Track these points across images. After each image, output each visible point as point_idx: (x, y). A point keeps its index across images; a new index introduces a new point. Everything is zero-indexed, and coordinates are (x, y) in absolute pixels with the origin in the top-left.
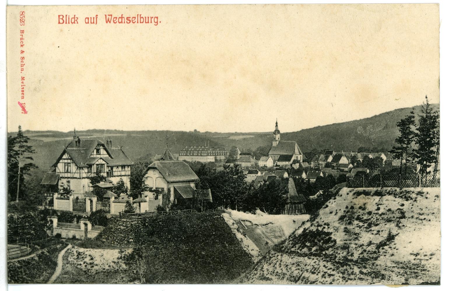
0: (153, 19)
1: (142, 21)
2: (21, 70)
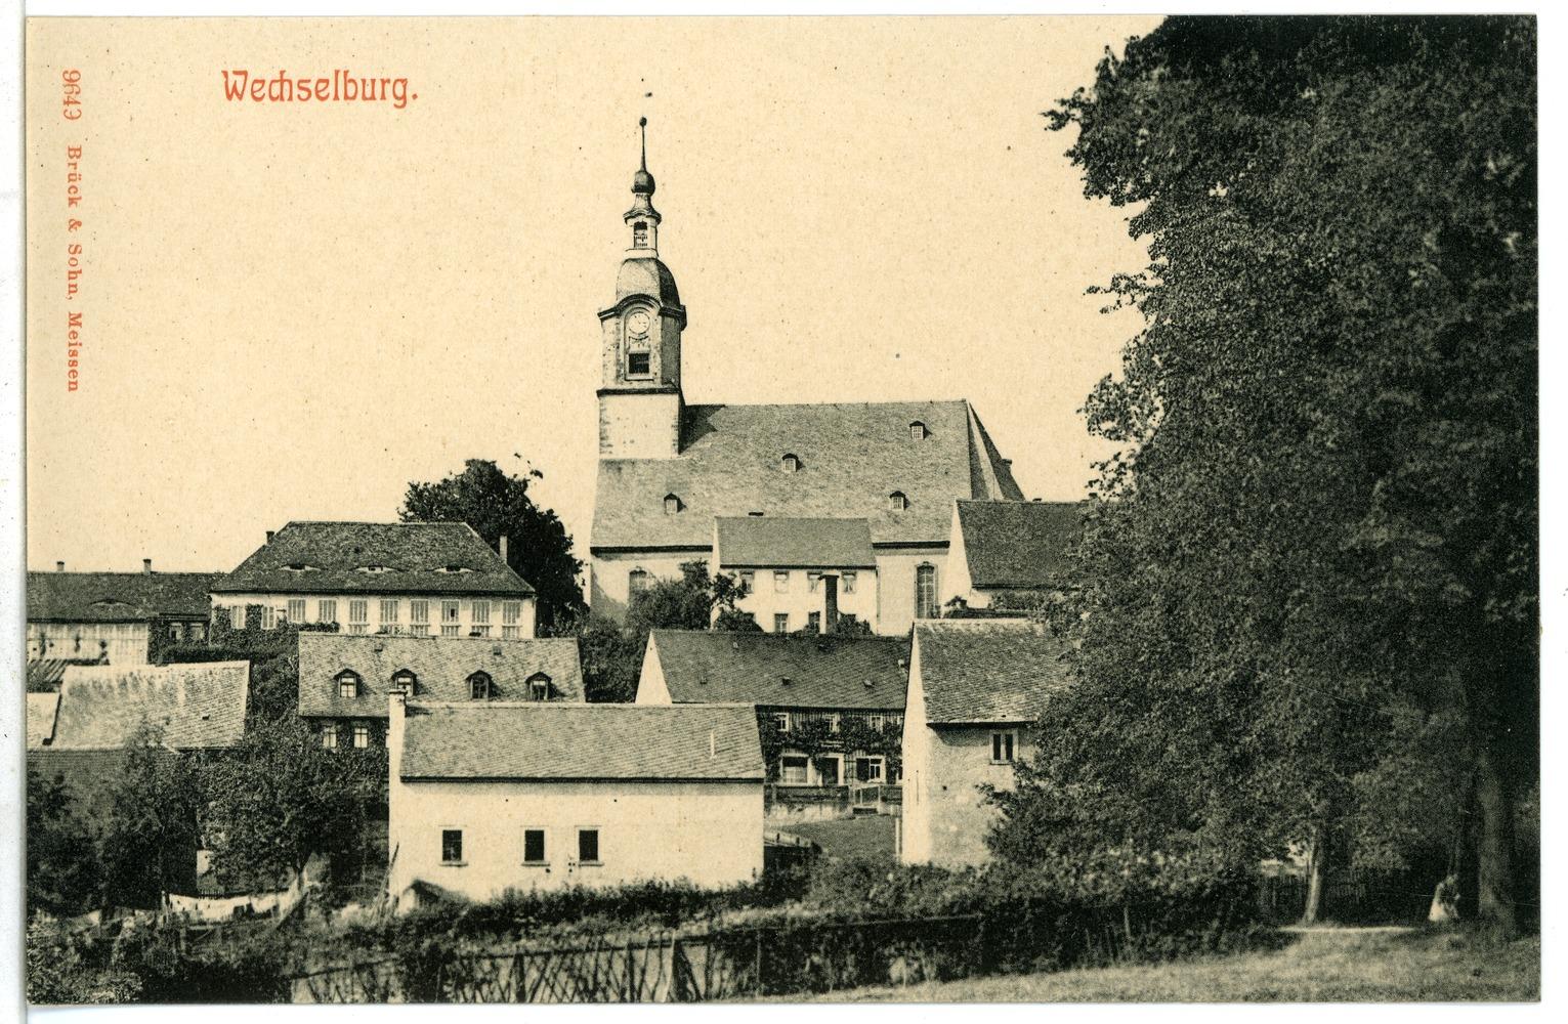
0: (389, 88)
2: (70, 292)
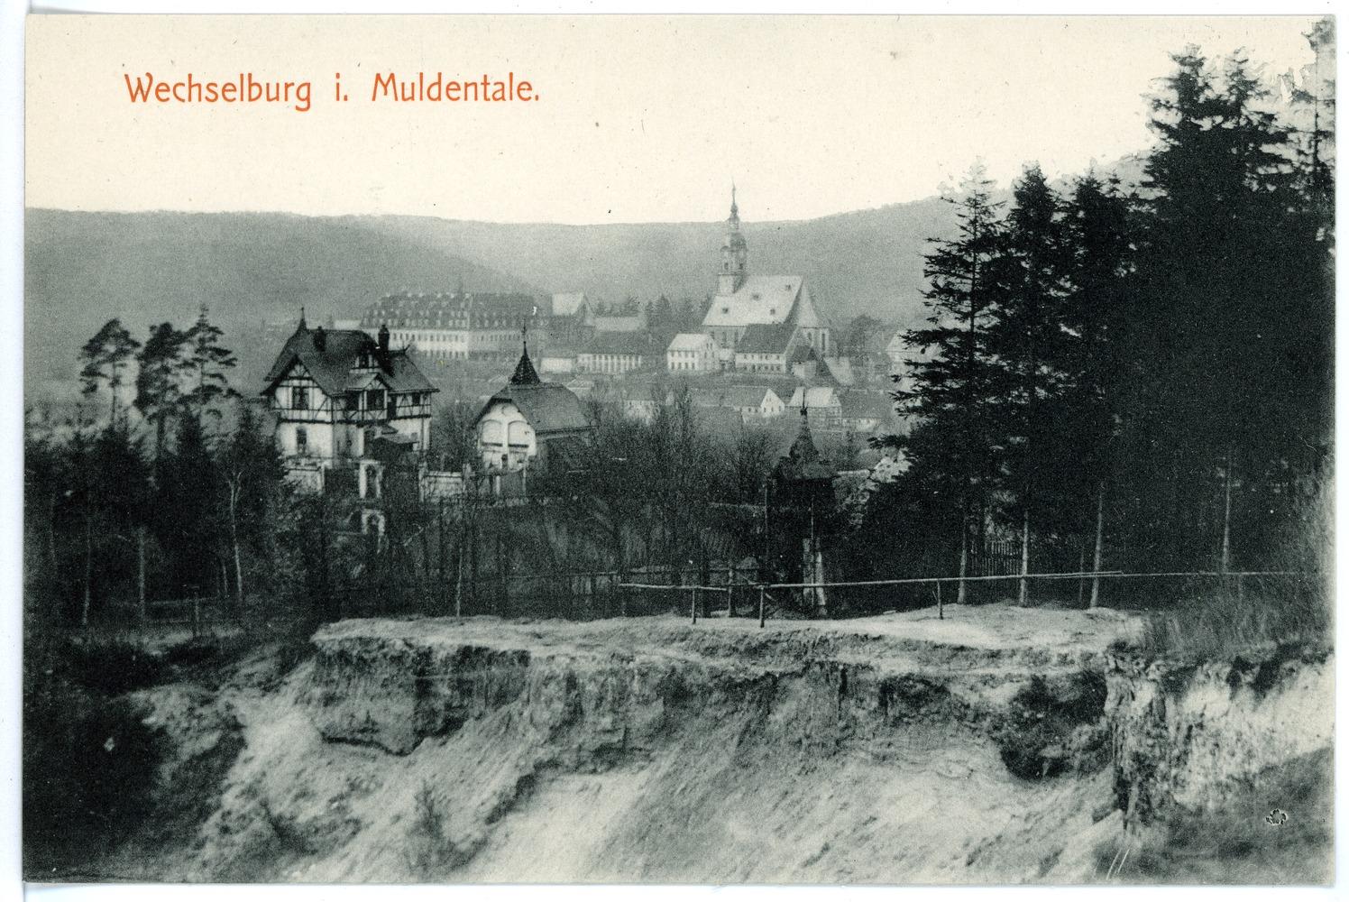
0: (292, 90)
1: (254, 95)
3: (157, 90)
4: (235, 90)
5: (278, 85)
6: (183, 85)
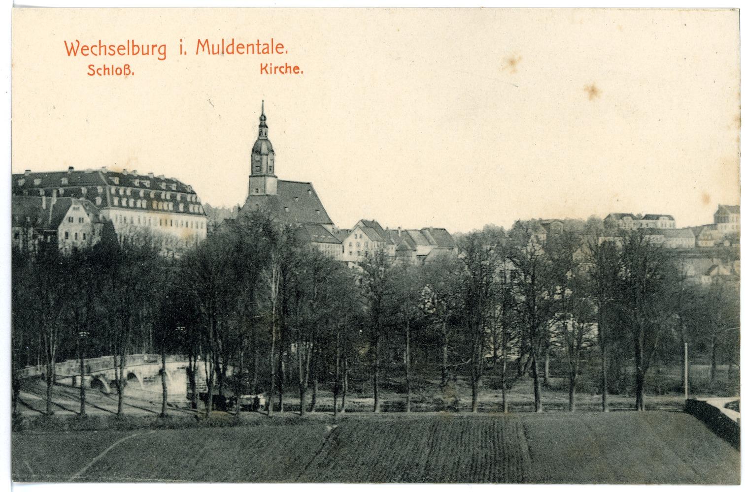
0: (156, 49)
3: (82, 50)
4: (124, 49)
5: (148, 46)
6: (96, 46)
